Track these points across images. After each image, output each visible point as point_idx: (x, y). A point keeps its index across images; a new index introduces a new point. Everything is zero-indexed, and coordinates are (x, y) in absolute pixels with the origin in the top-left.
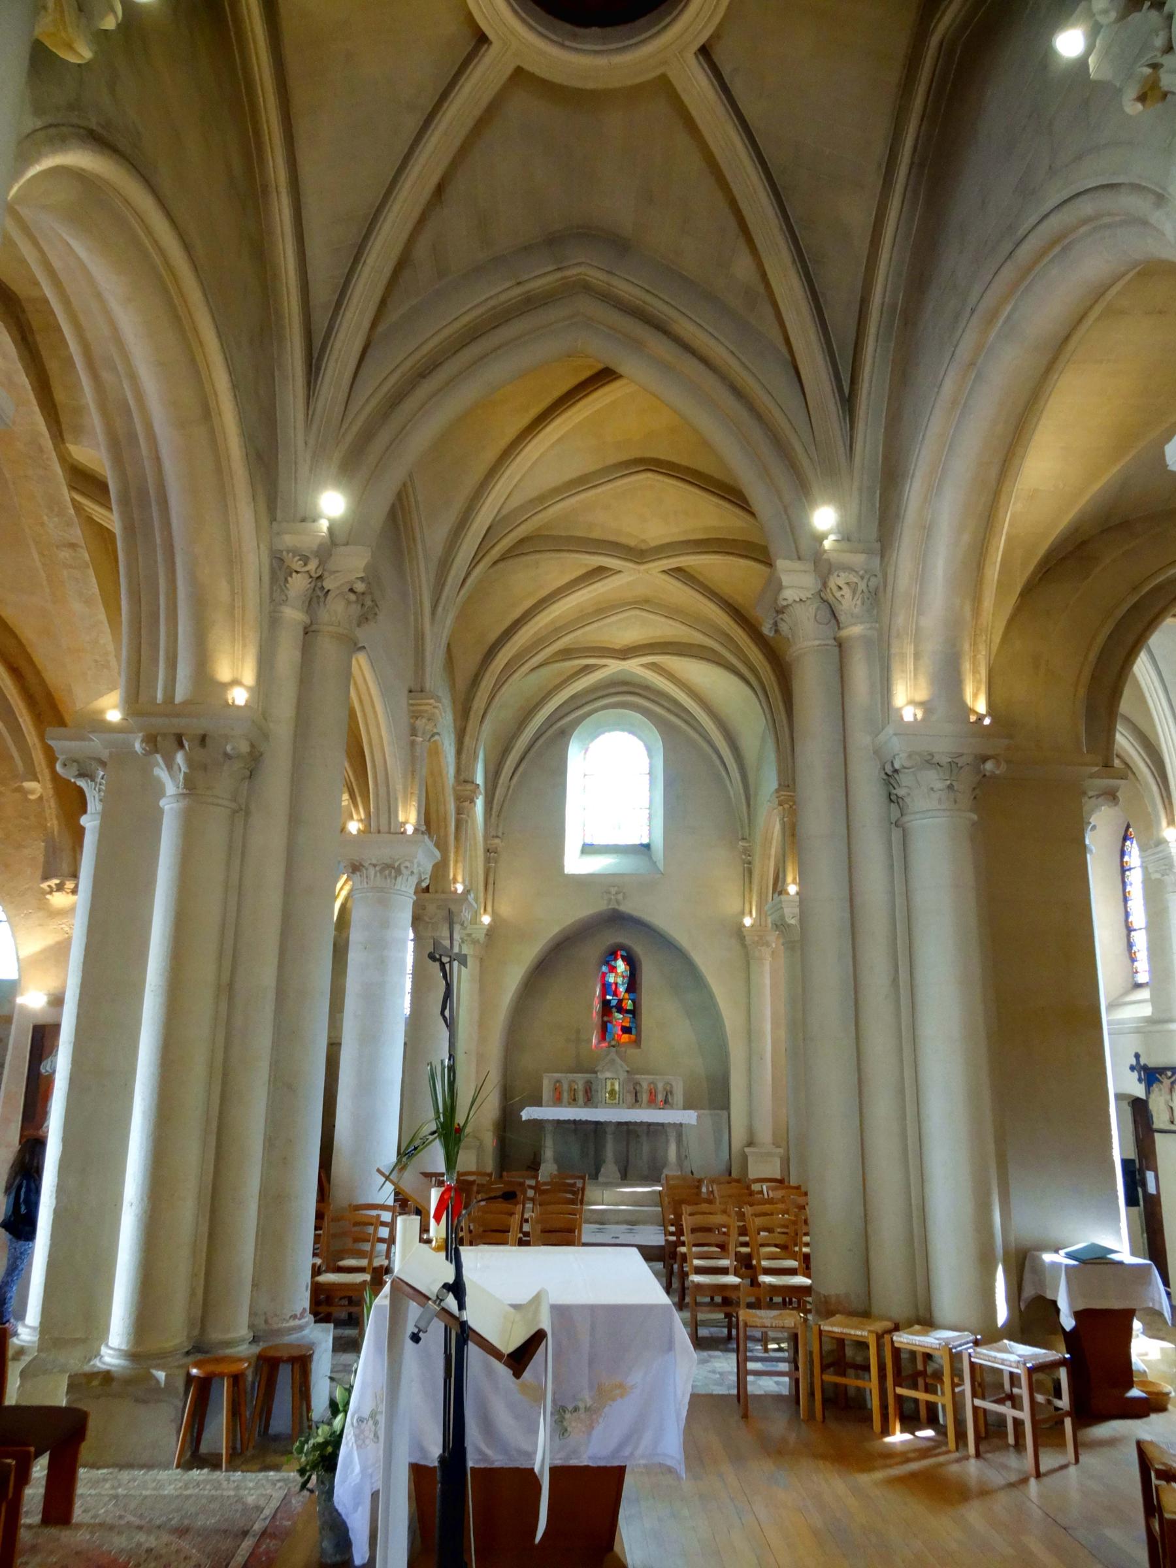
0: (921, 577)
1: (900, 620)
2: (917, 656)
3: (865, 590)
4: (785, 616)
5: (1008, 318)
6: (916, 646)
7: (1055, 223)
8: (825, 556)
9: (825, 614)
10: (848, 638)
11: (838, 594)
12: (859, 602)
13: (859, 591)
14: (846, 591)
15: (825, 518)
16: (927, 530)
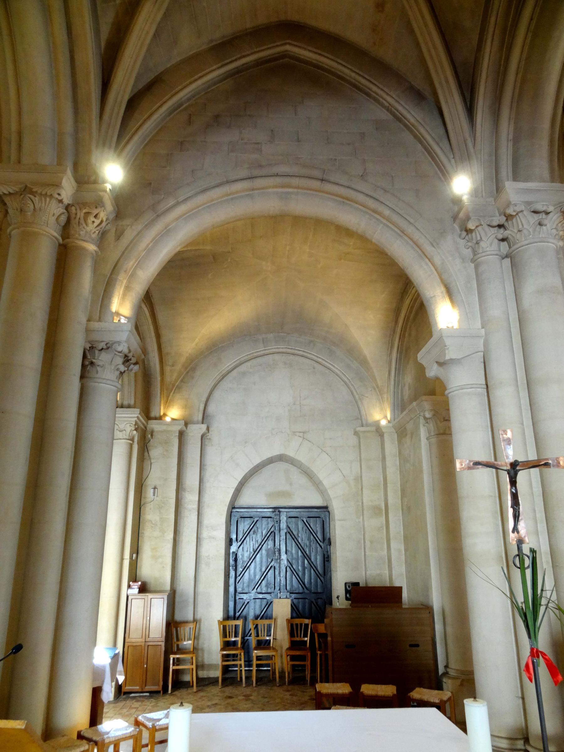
0: (150, 251)
1: (130, 264)
2: (128, 288)
3: (103, 228)
4: (36, 199)
5: (288, 193)
6: (129, 282)
7: (361, 198)
8: (102, 194)
9: (63, 219)
10: (84, 249)
11: (91, 218)
12: (97, 232)
13: (101, 226)
14: (97, 222)
15: (113, 173)
16: (167, 232)
